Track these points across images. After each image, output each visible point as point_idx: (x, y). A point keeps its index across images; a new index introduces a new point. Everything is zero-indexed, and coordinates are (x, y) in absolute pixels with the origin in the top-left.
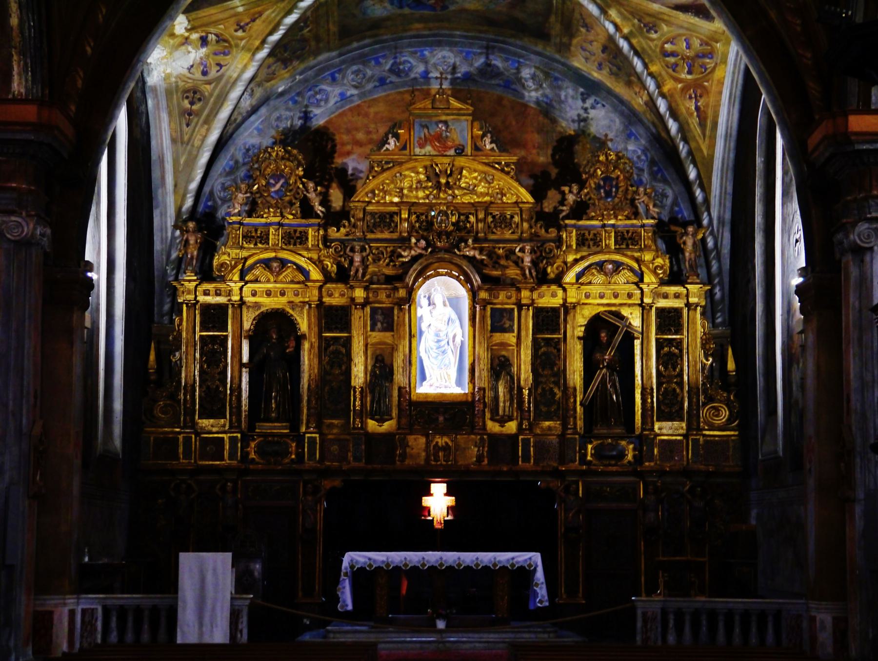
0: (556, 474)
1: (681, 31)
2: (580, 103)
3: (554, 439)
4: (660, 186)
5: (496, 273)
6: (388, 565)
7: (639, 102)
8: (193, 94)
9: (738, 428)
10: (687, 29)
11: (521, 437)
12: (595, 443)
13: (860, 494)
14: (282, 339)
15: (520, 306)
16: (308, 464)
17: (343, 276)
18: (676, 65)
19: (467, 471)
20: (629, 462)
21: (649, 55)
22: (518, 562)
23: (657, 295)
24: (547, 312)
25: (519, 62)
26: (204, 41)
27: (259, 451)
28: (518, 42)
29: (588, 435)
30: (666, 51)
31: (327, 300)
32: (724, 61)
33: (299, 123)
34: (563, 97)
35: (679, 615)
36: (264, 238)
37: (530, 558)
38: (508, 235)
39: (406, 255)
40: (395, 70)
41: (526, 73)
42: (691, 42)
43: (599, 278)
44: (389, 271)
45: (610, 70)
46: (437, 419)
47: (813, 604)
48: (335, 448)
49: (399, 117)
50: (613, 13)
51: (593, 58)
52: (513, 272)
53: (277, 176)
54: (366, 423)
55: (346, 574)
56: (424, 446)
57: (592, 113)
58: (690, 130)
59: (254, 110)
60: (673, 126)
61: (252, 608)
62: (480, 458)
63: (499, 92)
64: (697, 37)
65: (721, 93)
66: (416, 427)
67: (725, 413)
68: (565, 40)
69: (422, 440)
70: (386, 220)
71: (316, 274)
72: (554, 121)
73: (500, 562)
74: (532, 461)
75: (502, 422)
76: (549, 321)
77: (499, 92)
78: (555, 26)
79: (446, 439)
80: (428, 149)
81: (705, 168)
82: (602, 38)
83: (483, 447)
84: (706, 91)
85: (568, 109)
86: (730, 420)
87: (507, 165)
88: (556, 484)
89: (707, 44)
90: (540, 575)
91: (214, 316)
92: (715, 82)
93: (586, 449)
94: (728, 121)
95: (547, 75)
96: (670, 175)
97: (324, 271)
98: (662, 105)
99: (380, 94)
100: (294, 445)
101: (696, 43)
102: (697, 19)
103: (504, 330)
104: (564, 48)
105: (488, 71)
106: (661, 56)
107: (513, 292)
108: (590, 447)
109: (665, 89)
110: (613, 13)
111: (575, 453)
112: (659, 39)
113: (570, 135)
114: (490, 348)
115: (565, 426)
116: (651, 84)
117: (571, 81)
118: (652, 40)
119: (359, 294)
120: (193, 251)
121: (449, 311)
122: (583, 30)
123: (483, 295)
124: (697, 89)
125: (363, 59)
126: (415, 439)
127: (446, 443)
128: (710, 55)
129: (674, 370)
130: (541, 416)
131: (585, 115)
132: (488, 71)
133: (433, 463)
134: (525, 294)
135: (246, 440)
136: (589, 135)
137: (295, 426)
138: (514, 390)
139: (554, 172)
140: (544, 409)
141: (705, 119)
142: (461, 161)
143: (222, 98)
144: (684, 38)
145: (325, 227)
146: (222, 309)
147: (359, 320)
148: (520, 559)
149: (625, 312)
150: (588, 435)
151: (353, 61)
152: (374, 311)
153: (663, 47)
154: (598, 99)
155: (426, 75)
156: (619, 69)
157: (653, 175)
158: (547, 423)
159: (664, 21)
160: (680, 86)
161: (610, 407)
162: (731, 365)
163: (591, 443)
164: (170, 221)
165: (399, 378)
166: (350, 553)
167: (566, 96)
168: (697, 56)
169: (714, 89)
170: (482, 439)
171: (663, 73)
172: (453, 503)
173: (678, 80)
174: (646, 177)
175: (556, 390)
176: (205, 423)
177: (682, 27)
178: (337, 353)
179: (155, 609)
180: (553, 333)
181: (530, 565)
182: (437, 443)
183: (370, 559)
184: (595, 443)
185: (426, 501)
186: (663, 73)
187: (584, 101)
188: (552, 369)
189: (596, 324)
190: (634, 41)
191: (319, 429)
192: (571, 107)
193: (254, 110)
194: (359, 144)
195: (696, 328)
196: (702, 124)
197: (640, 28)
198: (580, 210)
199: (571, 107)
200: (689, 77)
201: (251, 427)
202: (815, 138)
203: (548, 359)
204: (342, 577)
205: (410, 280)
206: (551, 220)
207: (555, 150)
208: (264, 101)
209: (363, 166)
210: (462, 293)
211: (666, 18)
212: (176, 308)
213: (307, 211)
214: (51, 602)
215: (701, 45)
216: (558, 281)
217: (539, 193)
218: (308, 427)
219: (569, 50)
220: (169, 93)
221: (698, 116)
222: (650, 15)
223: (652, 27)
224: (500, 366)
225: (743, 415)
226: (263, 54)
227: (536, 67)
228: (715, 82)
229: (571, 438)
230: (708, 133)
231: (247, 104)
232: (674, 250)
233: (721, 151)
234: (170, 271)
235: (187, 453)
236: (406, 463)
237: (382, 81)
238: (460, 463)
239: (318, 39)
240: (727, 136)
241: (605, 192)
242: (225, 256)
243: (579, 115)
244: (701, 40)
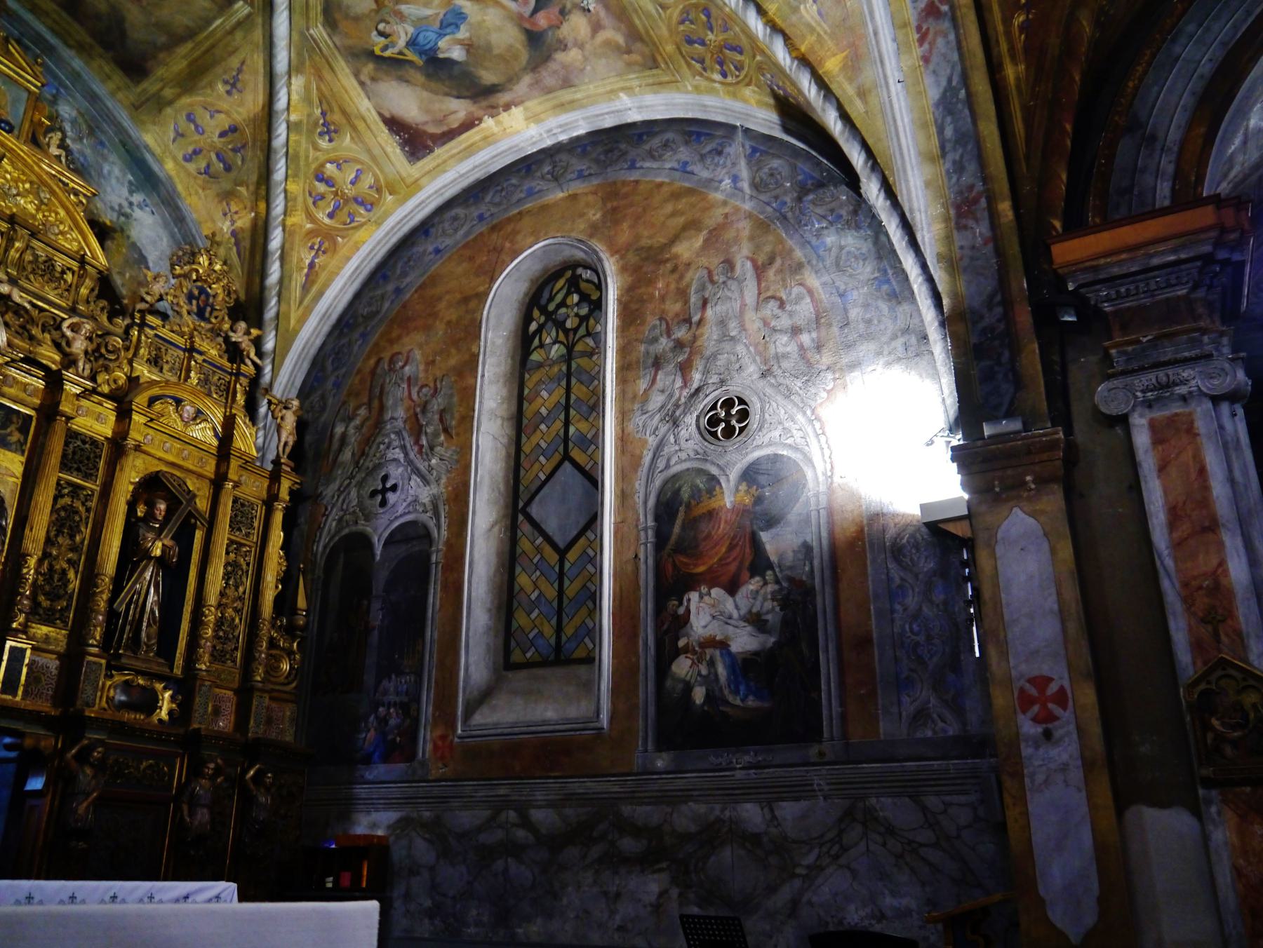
1: (364, 157)
2: (125, 192)
10: (373, 158)
18: (322, 197)
20: (160, 721)
21: (298, 166)
24: (84, 442)
25: (58, 90)
28: (77, 63)
30: (323, 173)
32: (379, 224)
34: (106, 170)
42: (362, 177)
45: (208, 166)
50: (298, 82)
51: (197, 137)
57: (138, 213)
58: (289, 289)
64: (375, 175)
65: (348, 259)
68: (168, 93)
74: (20, 692)
81: (285, 342)
85: (109, 189)
87: (76, 194)
89: (379, 191)
92: (351, 243)
94: (336, 297)
95: (91, 132)
101: (368, 180)
102: (398, 150)
104: (157, 104)
106: (312, 177)
109: (289, 221)
112: (327, 151)
113: (105, 224)
117: (120, 158)
118: (316, 148)
122: (221, 88)
124: (325, 241)
128: (368, 205)
129: (237, 588)
131: (129, 211)
136: (128, 237)
140: (46, 603)
141: (313, 282)
144: (359, 167)
149: (191, 484)
153: (323, 165)
154: (148, 201)
156: (228, 168)
159: (354, 128)
160: (309, 226)
162: (302, 602)
167: (110, 173)
168: (356, 200)
169: (343, 252)
171: (300, 199)
173: (311, 217)
175: (71, 575)
177: (369, 151)
180: (87, 477)
186: (300, 199)
187: (131, 192)
188: (72, 537)
189: (151, 486)
190: (293, 137)
192: (113, 190)
196: (306, 288)
197: (316, 124)
199: (113, 190)
200: (327, 221)
211: (361, 126)
215: (371, 187)
219: (160, 111)
221: (307, 276)
222: (344, 113)
223: (330, 131)
227: (79, 113)
228: (351, 243)
229: (95, 663)
230: (306, 302)
240: (325, 316)
241: (198, 306)
243: (120, 205)
244: (377, 180)
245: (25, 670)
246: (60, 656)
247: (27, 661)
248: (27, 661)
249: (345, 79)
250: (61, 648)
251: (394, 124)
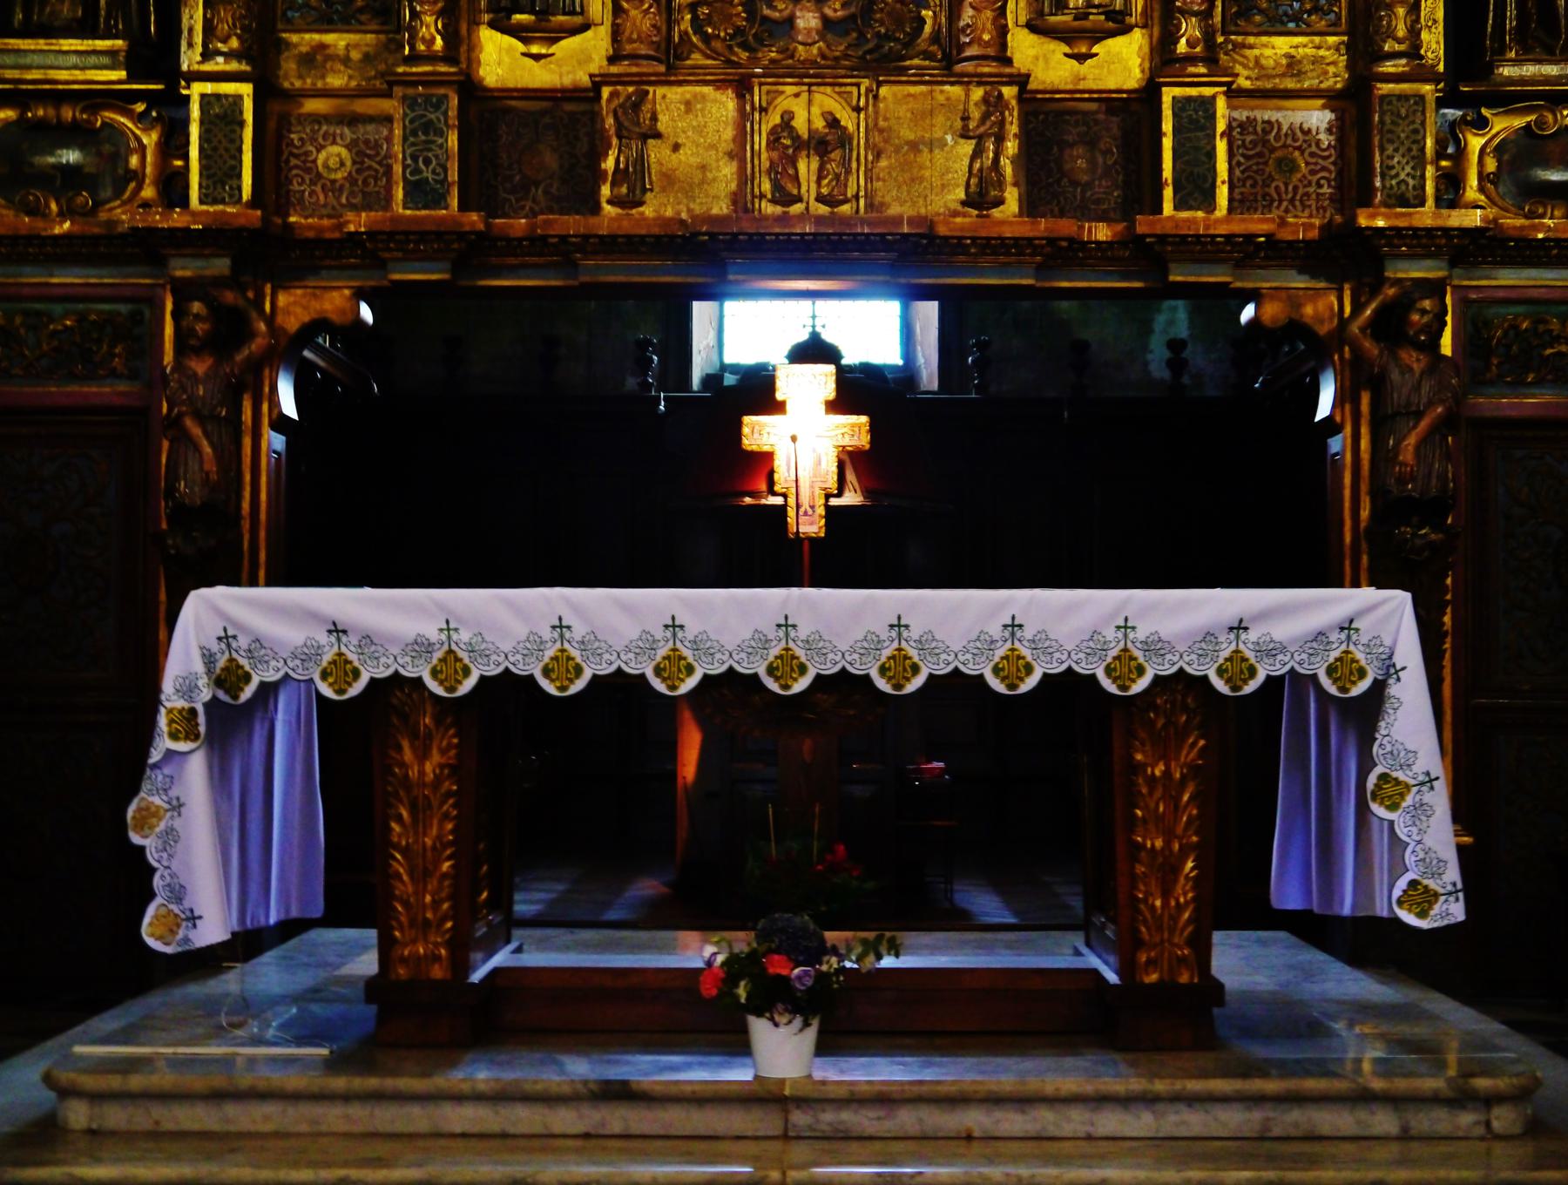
6: (451, 666)
11: (1168, 95)
12: (1503, 124)
22: (1270, 650)
29: (1469, 80)
37: (1347, 626)
46: (790, 21)
48: (333, 156)
54: (473, 47)
55: (186, 724)
56: (729, 133)
62: (982, 196)
66: (697, 58)
69: (724, 105)
73: (1155, 647)
79: (827, 100)
83: (1000, 139)
90: (1411, 729)
93: (1461, 153)
100: (150, 139)
108: (1475, 143)
111: (1420, 161)
115: (1364, 50)
126: (688, 105)
127: (833, 122)
133: (769, 209)
137: (154, 57)
148: (1283, 631)
158: (1282, 44)
163: (1481, 124)
166: (204, 591)
170: (994, 104)
172: (864, 441)
181: (1344, 669)
182: (788, 117)
183: (337, 630)
184: (1503, 124)
191: (261, 60)
204: (164, 743)
218: (207, 55)
229: (1402, 97)
236: (648, 211)
238: (894, 210)
245: (1221, 147)
246: (1332, 99)
247: (1221, 126)
248: (1221, 126)
250: (1336, 76)
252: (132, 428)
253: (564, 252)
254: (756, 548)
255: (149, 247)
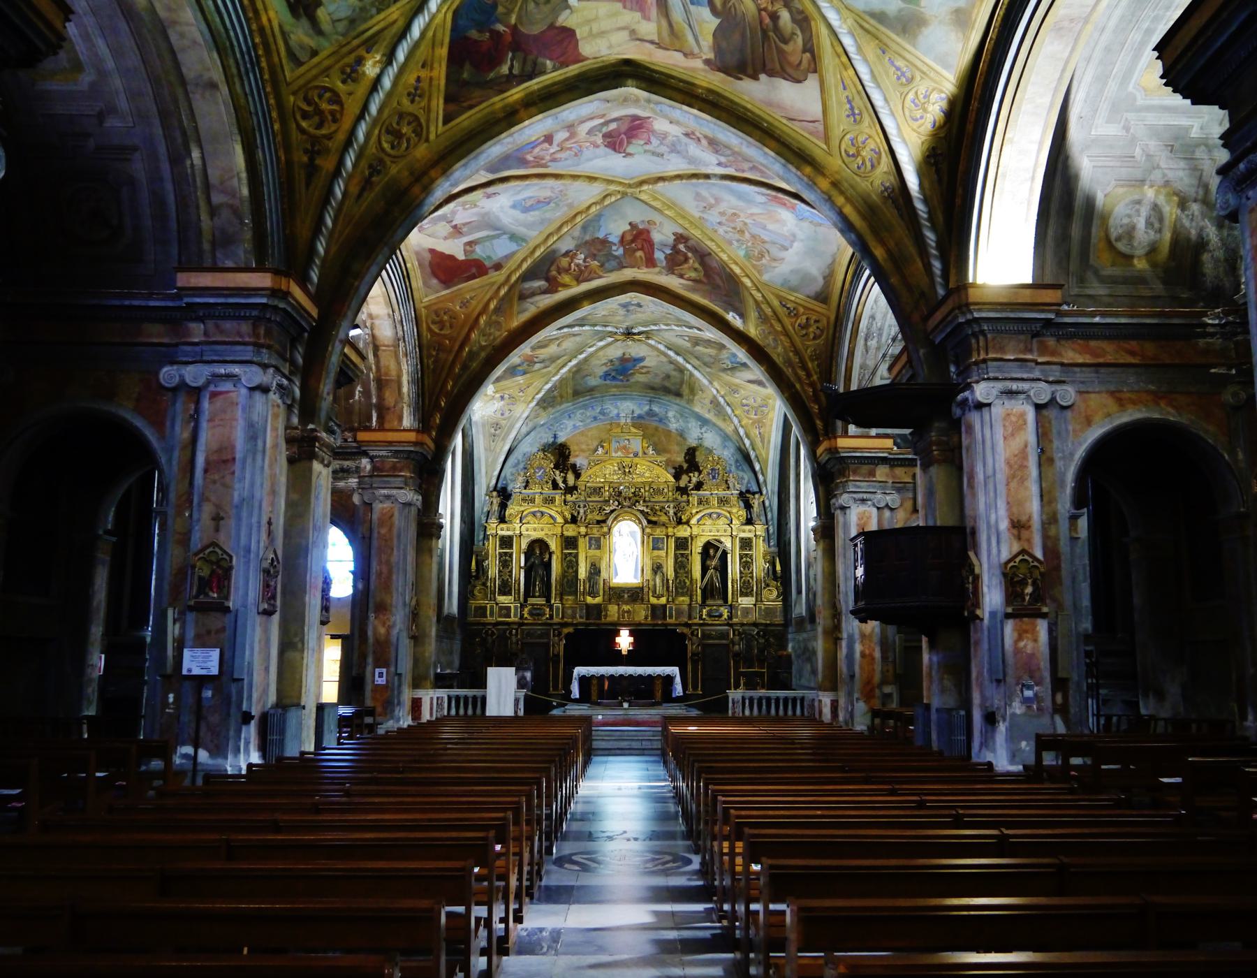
0: (687, 625)
3: (685, 607)
4: (741, 474)
5: (654, 519)
7: (729, 430)
8: (497, 426)
9: (783, 600)
13: (845, 635)
14: (541, 554)
15: (668, 537)
16: (556, 620)
17: (574, 520)
19: (640, 624)
23: (739, 530)
26: (502, 398)
27: (530, 613)
29: (703, 604)
31: (566, 533)
32: (773, 408)
33: (551, 440)
35: (751, 699)
36: (533, 501)
38: (661, 499)
39: (608, 509)
40: (602, 413)
41: (671, 414)
43: (709, 522)
44: (599, 518)
47: (820, 693)
48: (569, 612)
49: (604, 436)
50: (716, 384)
52: (664, 518)
53: (540, 468)
59: (528, 434)
60: (747, 442)
61: (526, 697)
62: (646, 618)
63: (655, 424)
67: (775, 593)
70: (597, 491)
71: (560, 520)
72: (685, 439)
75: (658, 597)
76: (682, 544)
77: (655, 424)
78: (685, 390)
80: (619, 454)
82: (711, 397)
84: (764, 425)
86: (778, 596)
88: (686, 630)
90: (678, 679)
91: (506, 542)
95: (682, 416)
96: (746, 467)
97: (564, 517)
98: (741, 432)
99: (595, 424)
101: (759, 400)
103: (659, 549)
104: (690, 401)
105: (651, 413)
107: (664, 529)
110: (716, 384)
114: (652, 558)
116: (736, 421)
119: (583, 530)
120: (496, 507)
121: (631, 540)
123: (648, 530)
124: (759, 423)
125: (585, 407)
128: (766, 406)
130: (678, 594)
132: (651, 413)
134: (670, 530)
135: (522, 606)
137: (548, 600)
138: (665, 581)
139: (685, 466)
142: (636, 460)
143: (512, 427)
145: (565, 494)
146: (510, 538)
147: (582, 544)
150: (703, 604)
151: (580, 408)
152: (590, 539)
155: (618, 415)
157: (737, 467)
161: (715, 591)
162: (778, 568)
164: (484, 491)
165: (604, 575)
174: (733, 468)
176: (501, 599)
178: (571, 561)
179: (475, 698)
185: (618, 640)
189: (708, 546)
191: (561, 600)
193: (528, 434)
194: (583, 451)
195: (760, 550)
196: (762, 441)
198: (699, 486)
201: (526, 601)
202: (820, 451)
203: (682, 565)
205: (609, 522)
206: (683, 491)
207: (686, 454)
208: (534, 428)
209: (585, 462)
210: (636, 529)
212: (486, 537)
213: (555, 486)
214: (420, 693)
216: (687, 523)
217: (677, 477)
220: (483, 425)
223: (735, 392)
224: (657, 568)
225: (785, 595)
226: (534, 403)
231: (524, 430)
232: (748, 506)
233: (773, 456)
234: (484, 519)
235: (492, 615)
237: (595, 418)
239: (562, 397)
242: (512, 509)
249: (727, 377)
251: (750, 382)
252: (548, 645)
253: (598, 625)
254: (616, 658)
255: (551, 625)
